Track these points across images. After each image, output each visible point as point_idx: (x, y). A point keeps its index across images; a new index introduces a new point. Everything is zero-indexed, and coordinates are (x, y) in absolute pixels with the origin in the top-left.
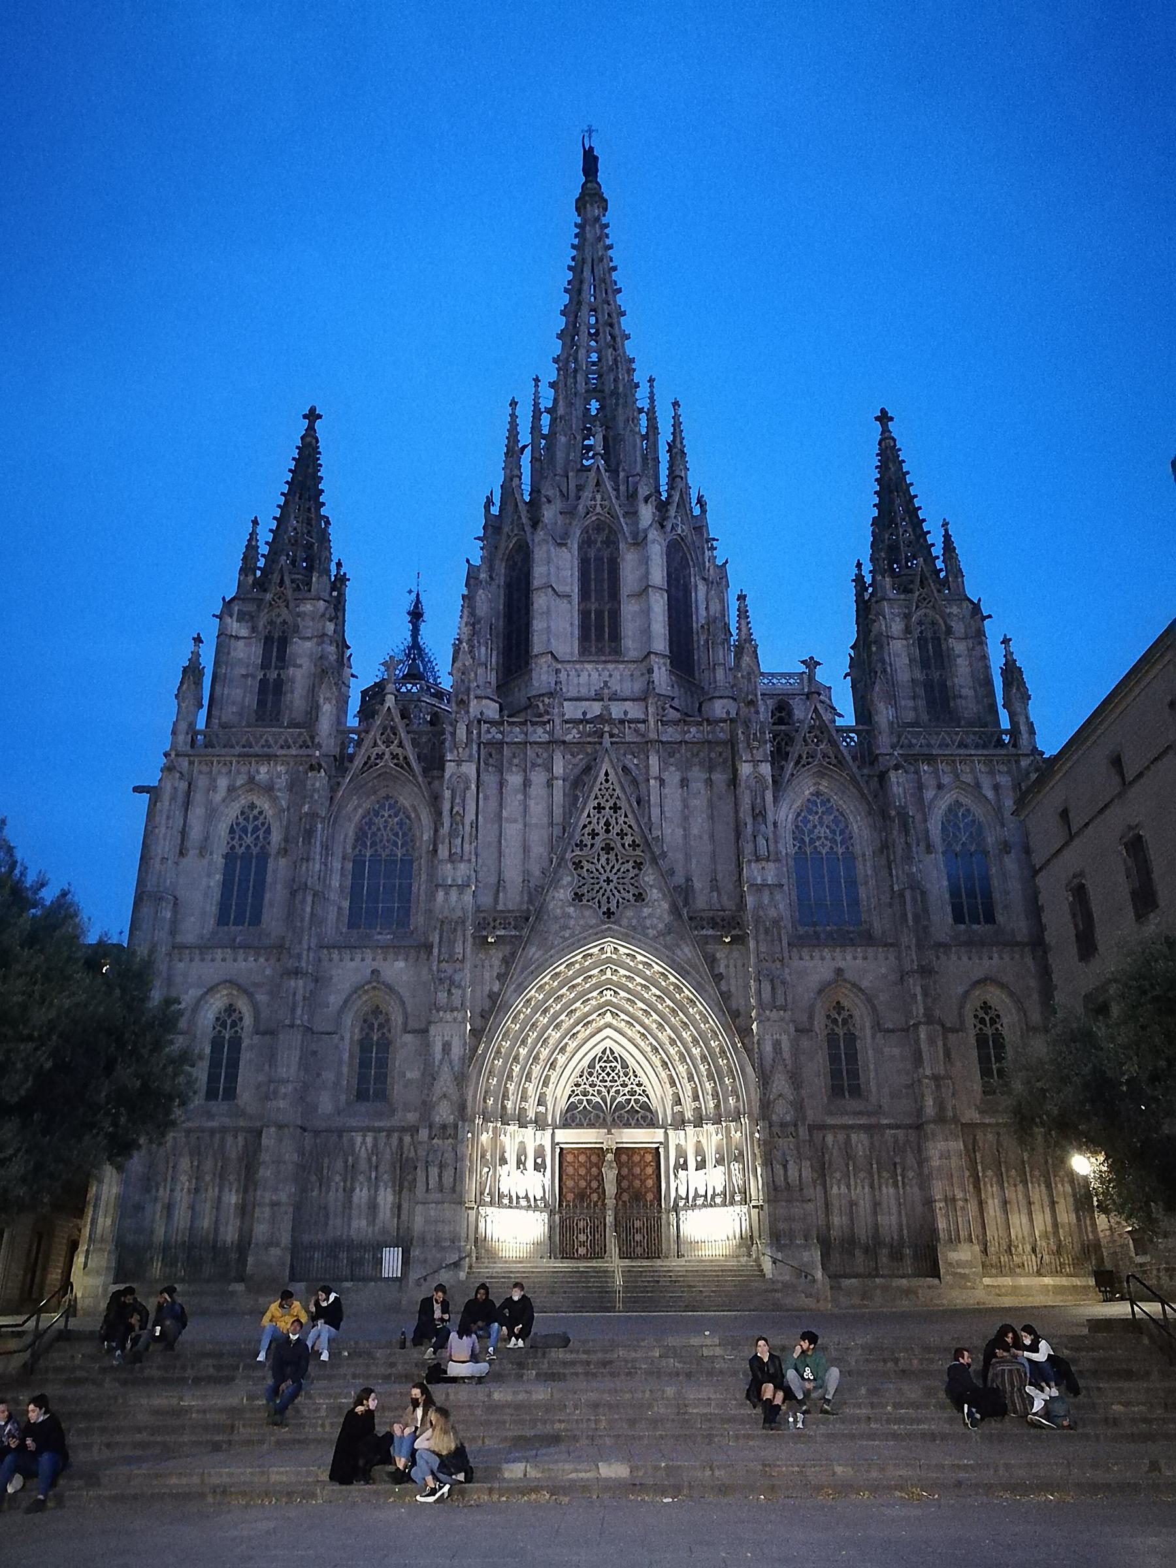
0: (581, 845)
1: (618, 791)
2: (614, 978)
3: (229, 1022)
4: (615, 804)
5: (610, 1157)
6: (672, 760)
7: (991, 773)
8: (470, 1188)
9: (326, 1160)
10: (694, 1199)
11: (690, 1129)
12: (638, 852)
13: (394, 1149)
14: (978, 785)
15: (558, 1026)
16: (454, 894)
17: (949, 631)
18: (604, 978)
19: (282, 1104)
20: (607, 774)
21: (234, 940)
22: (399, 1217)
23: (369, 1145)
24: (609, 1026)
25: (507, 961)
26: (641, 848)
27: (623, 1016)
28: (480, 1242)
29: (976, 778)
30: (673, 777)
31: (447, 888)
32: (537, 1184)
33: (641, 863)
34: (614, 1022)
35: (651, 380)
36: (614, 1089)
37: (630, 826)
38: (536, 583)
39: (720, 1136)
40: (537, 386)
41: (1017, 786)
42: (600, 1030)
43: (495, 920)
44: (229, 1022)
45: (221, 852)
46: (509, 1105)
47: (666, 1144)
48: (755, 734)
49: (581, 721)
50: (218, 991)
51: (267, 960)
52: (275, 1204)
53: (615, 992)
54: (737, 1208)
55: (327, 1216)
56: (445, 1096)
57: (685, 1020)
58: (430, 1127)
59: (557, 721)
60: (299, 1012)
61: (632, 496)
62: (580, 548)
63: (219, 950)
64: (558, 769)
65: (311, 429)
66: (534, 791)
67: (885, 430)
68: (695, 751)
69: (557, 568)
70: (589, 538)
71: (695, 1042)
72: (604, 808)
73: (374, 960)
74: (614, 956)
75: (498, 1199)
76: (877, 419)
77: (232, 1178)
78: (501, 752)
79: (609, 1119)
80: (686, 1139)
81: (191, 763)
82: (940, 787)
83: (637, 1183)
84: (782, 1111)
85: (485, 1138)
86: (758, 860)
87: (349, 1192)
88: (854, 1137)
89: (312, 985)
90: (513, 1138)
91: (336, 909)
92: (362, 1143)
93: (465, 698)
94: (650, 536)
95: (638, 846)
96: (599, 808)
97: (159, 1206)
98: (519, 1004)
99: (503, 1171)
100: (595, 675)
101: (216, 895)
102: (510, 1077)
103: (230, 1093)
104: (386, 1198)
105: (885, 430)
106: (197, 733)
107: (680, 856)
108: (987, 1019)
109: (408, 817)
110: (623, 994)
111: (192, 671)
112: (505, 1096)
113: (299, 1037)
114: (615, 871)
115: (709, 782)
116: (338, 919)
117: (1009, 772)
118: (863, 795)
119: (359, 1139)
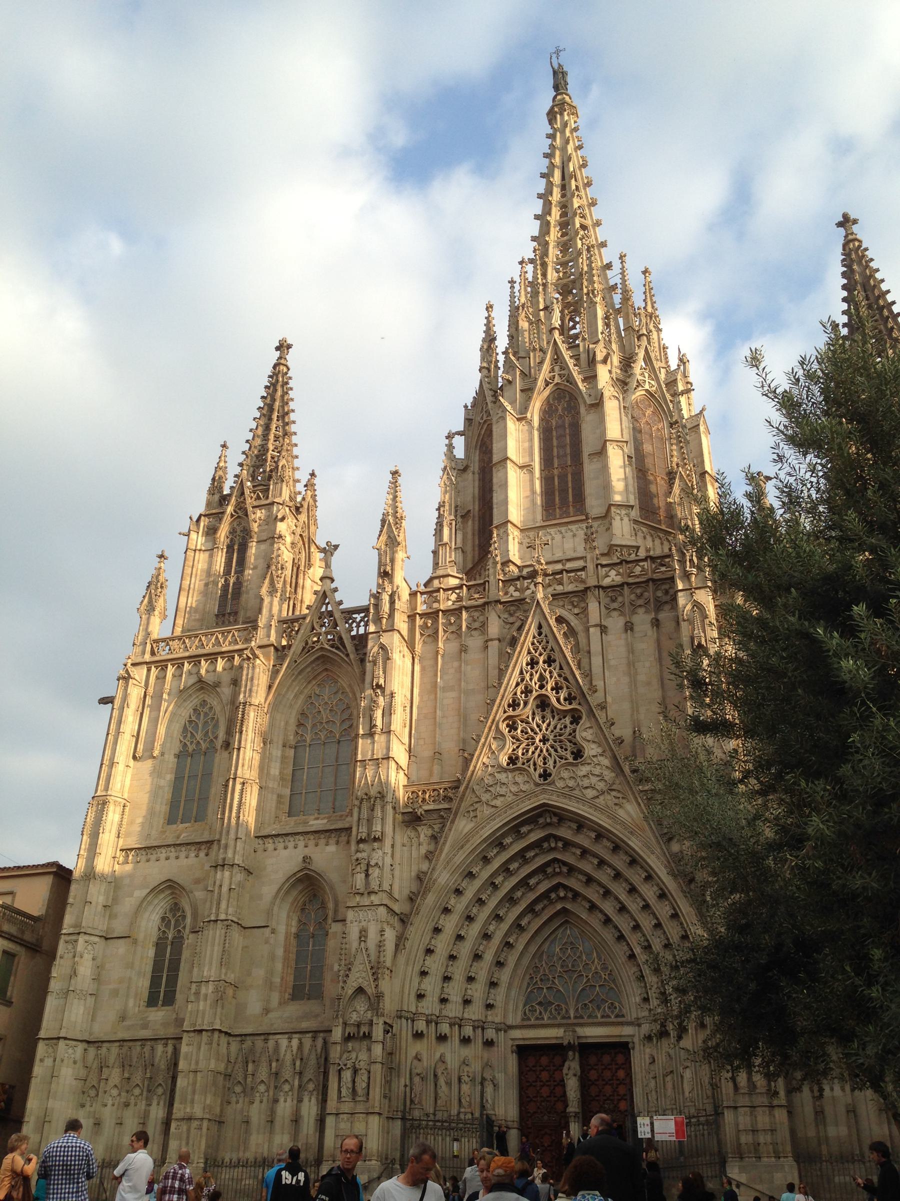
4: (549, 657)
6: (615, 605)
13: (319, 1050)
20: (540, 627)
21: (178, 837)
23: (295, 1048)
25: (434, 838)
26: (577, 701)
30: (616, 623)
33: (580, 718)
35: (621, 257)
37: (566, 679)
38: (495, 459)
40: (512, 287)
43: (424, 792)
45: (173, 752)
48: (691, 560)
49: (518, 579)
50: (162, 891)
51: (207, 855)
55: (247, 1132)
56: (360, 990)
58: (345, 1024)
60: (223, 905)
61: (592, 362)
62: (541, 420)
63: (164, 851)
65: (280, 358)
68: (638, 591)
69: (519, 441)
72: (537, 663)
73: (306, 847)
76: (840, 225)
77: (160, 1091)
78: (436, 621)
81: (149, 670)
83: (608, 1090)
89: (239, 877)
91: (275, 797)
93: (388, 569)
94: (607, 394)
95: (575, 698)
96: (533, 663)
100: (558, 537)
101: (167, 794)
103: (169, 1000)
104: (309, 1109)
106: (156, 641)
107: (626, 706)
111: (155, 586)
113: (223, 931)
114: (551, 727)
115: (656, 623)
116: (277, 808)
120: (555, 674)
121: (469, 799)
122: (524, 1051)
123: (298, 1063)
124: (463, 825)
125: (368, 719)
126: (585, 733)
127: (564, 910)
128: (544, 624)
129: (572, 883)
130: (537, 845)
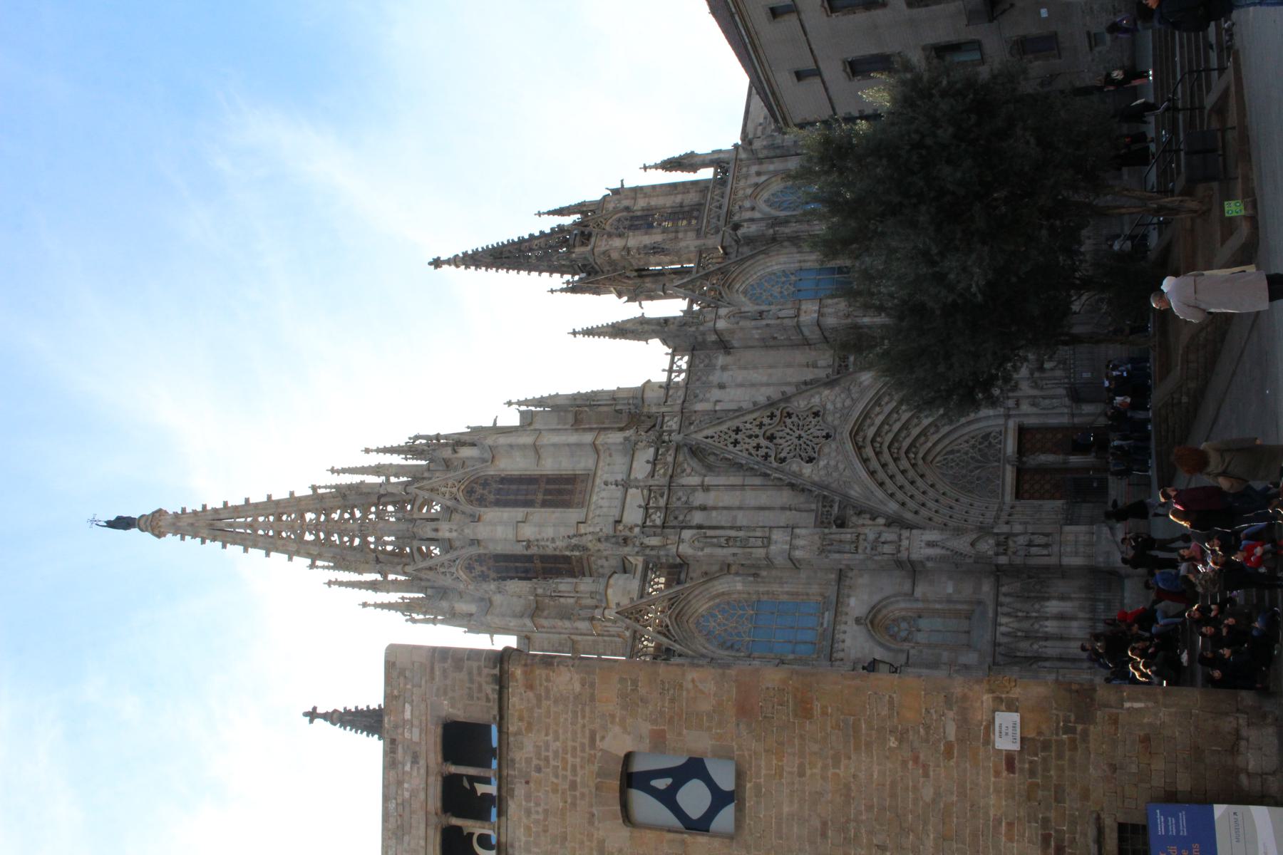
0: (766, 456)
1: (724, 427)
6: (701, 396)
7: (747, 177)
9: (1018, 654)
12: (778, 413)
14: (757, 185)
16: (800, 542)
17: (627, 209)
25: (859, 513)
29: (750, 186)
30: (716, 394)
31: (793, 547)
41: (760, 161)
56: (972, 544)
58: (997, 554)
59: (651, 482)
64: (694, 480)
66: (710, 503)
67: (449, 262)
70: (477, 500)
82: (753, 209)
86: (797, 316)
92: (1007, 624)
100: (603, 494)
105: (449, 262)
109: (718, 605)
115: (724, 368)
117: (748, 166)
118: (752, 257)
119: (1003, 629)
120: (748, 426)
121: (834, 485)
122: (1018, 495)
123: (1020, 614)
124: (855, 492)
125: (753, 550)
126: (800, 404)
127: (924, 458)
128: (706, 433)
129: (906, 444)
130: (877, 454)
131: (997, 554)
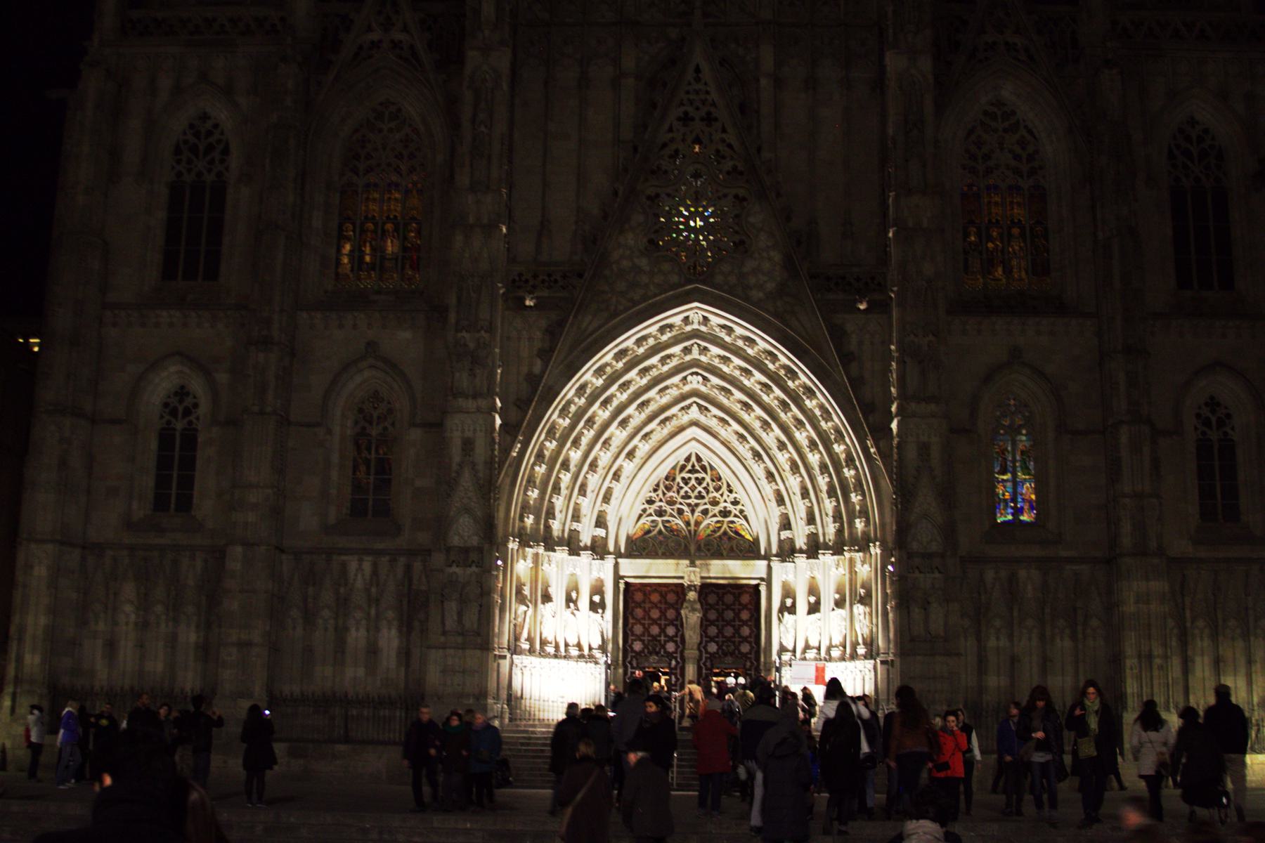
1: (714, 96)
2: (703, 358)
3: (181, 409)
4: (709, 113)
5: (692, 595)
8: (501, 633)
9: (311, 590)
10: (804, 652)
11: (801, 560)
15: (624, 423)
18: (688, 358)
19: (251, 517)
22: (408, 666)
24: (695, 423)
25: (553, 333)
27: (715, 411)
28: (513, 700)
32: (594, 628)
34: (702, 419)
36: (701, 508)
37: (730, 146)
39: (841, 570)
42: (682, 429)
43: (535, 276)
44: (181, 409)
46: (556, 526)
47: (768, 581)
52: (245, 645)
53: (705, 378)
54: (859, 664)
57: (801, 417)
71: (813, 445)
72: (693, 119)
74: (703, 329)
75: (539, 648)
79: (693, 548)
80: (793, 574)
84: (926, 537)
85: (522, 568)
87: (341, 634)
88: (1022, 574)
90: (559, 568)
92: (359, 570)
97: (100, 642)
98: (569, 391)
99: (546, 610)
102: (556, 489)
103: (185, 504)
104: (390, 639)
108: (1214, 419)
110: (715, 380)
112: (551, 514)
119: (353, 565)
128: (705, 67)
131: (448, 550)
